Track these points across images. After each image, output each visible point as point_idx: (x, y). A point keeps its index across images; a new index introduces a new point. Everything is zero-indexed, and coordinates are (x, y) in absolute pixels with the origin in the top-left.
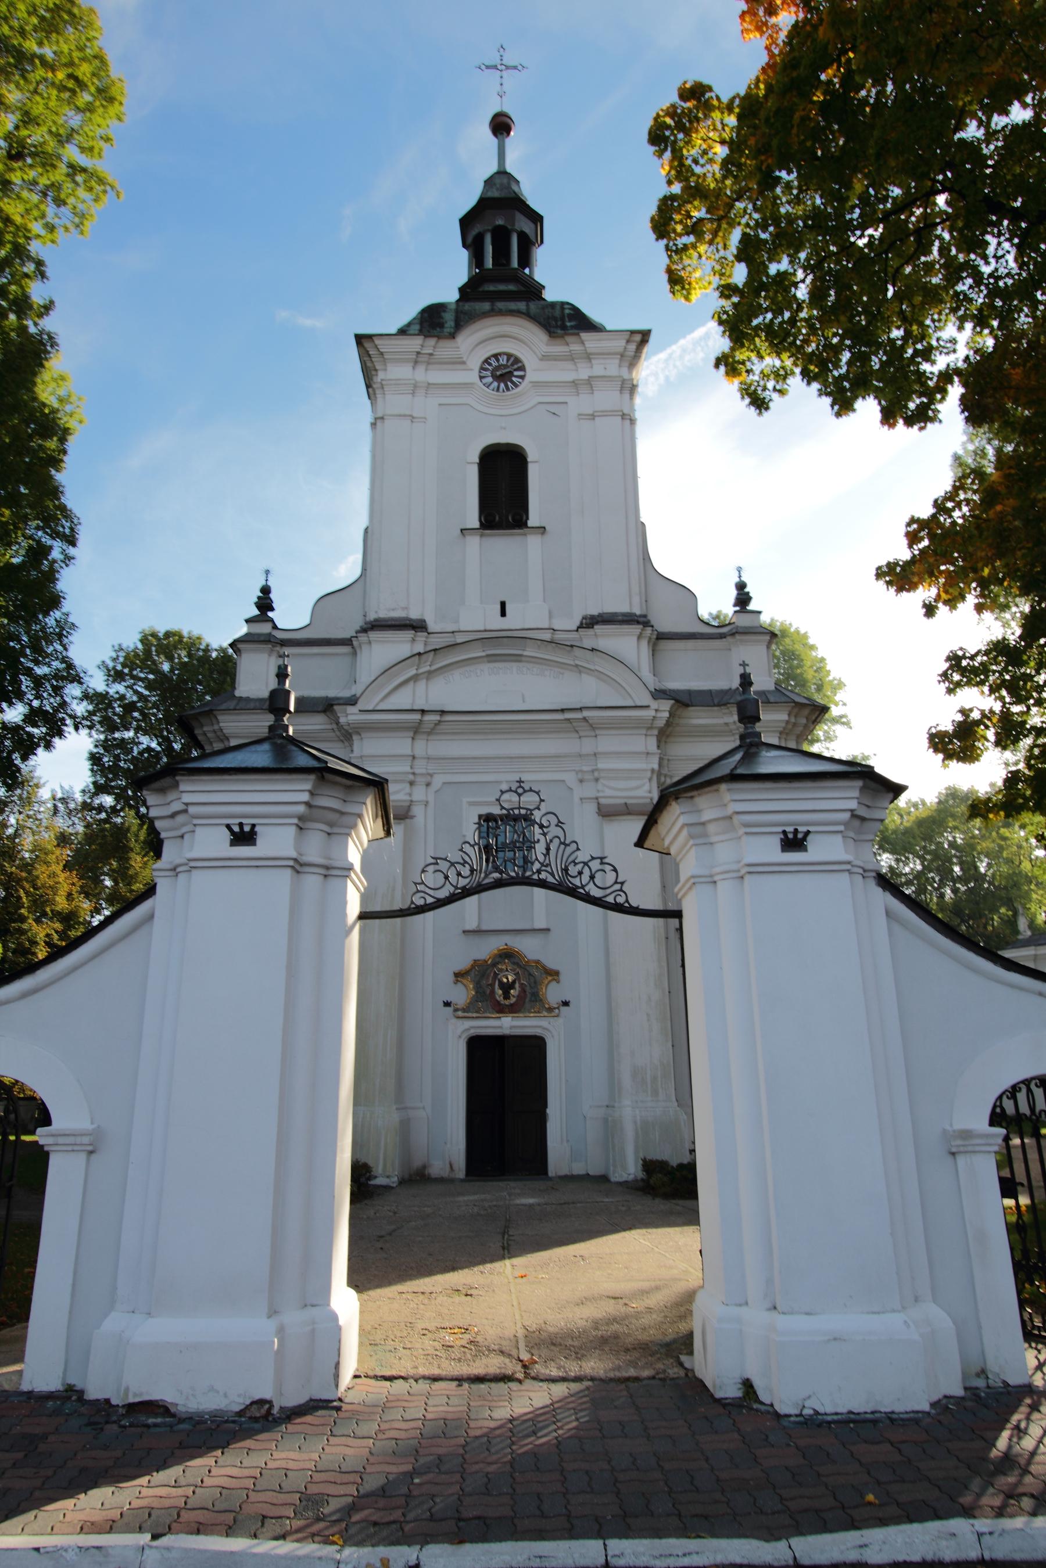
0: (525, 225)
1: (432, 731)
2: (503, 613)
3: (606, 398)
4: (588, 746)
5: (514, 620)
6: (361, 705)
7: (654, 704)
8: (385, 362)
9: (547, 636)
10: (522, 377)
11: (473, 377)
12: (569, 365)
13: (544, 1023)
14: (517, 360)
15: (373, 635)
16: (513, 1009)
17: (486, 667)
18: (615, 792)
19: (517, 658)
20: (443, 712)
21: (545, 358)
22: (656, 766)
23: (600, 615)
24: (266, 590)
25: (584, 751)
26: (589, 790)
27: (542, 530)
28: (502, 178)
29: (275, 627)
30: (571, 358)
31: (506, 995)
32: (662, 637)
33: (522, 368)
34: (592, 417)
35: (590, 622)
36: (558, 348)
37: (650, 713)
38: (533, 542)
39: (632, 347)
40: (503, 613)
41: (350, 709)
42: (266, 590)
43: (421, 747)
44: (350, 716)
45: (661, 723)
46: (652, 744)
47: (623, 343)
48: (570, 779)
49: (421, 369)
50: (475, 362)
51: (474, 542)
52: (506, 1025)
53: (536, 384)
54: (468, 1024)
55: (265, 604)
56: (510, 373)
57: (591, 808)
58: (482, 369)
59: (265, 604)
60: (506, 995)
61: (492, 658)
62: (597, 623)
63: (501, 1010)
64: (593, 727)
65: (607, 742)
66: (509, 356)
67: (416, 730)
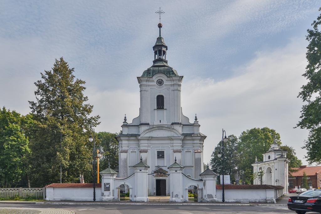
0: (164, 49)
1: (151, 140)
2: (160, 122)
3: (176, 87)
4: (172, 142)
5: (161, 123)
6: (141, 136)
7: (181, 137)
8: (142, 81)
9: (166, 126)
10: (163, 83)
11: (155, 83)
12: (170, 81)
13: (166, 178)
14: (162, 80)
15: (142, 126)
16: (162, 176)
17: (158, 130)
18: (175, 148)
19: (162, 129)
20: (152, 137)
21: (166, 80)
22: (181, 145)
23: (174, 123)
24: (125, 117)
25: (172, 143)
26: (172, 148)
27: (166, 109)
28: (159, 39)
29: (127, 123)
30: (171, 80)
31: (161, 174)
32: (184, 125)
33: (163, 82)
34: (174, 91)
35: (173, 124)
36: (169, 79)
37: (181, 138)
38: (165, 111)
39: (180, 79)
40: (160, 122)
41: (140, 137)
42: (125, 117)
43: (149, 142)
44: (139, 138)
45: (182, 139)
46: (181, 142)
47: (179, 78)
48: (169, 146)
49: (147, 82)
50: (156, 81)
51: (156, 111)
52: (161, 178)
53: (165, 85)
54: (156, 178)
55: (125, 120)
56: (161, 82)
57: (172, 151)
58: (157, 82)
59: (125, 120)
60: (161, 174)
61: (158, 129)
62: (174, 124)
63: (160, 176)
64: (173, 140)
65: (175, 142)
66: (161, 79)
67: (148, 140)
